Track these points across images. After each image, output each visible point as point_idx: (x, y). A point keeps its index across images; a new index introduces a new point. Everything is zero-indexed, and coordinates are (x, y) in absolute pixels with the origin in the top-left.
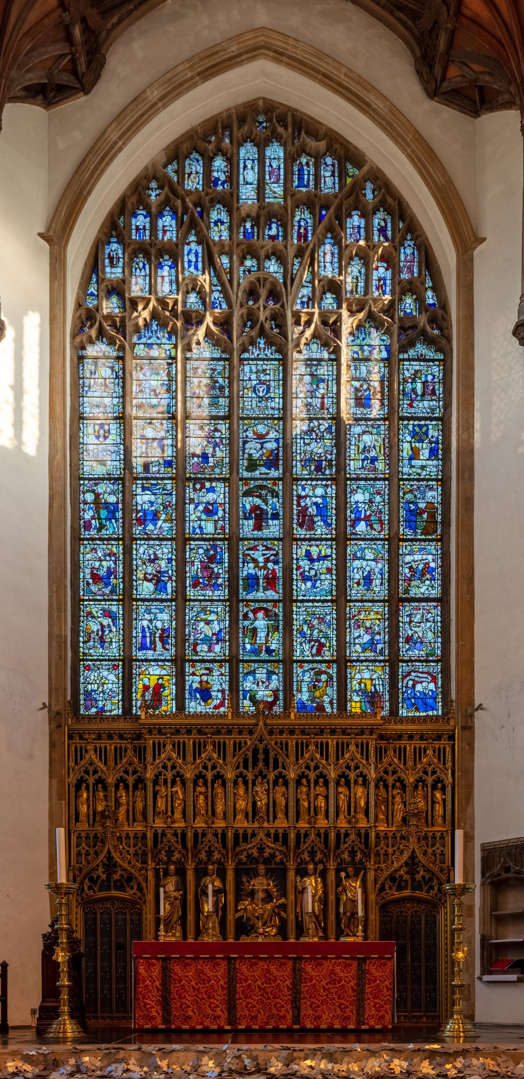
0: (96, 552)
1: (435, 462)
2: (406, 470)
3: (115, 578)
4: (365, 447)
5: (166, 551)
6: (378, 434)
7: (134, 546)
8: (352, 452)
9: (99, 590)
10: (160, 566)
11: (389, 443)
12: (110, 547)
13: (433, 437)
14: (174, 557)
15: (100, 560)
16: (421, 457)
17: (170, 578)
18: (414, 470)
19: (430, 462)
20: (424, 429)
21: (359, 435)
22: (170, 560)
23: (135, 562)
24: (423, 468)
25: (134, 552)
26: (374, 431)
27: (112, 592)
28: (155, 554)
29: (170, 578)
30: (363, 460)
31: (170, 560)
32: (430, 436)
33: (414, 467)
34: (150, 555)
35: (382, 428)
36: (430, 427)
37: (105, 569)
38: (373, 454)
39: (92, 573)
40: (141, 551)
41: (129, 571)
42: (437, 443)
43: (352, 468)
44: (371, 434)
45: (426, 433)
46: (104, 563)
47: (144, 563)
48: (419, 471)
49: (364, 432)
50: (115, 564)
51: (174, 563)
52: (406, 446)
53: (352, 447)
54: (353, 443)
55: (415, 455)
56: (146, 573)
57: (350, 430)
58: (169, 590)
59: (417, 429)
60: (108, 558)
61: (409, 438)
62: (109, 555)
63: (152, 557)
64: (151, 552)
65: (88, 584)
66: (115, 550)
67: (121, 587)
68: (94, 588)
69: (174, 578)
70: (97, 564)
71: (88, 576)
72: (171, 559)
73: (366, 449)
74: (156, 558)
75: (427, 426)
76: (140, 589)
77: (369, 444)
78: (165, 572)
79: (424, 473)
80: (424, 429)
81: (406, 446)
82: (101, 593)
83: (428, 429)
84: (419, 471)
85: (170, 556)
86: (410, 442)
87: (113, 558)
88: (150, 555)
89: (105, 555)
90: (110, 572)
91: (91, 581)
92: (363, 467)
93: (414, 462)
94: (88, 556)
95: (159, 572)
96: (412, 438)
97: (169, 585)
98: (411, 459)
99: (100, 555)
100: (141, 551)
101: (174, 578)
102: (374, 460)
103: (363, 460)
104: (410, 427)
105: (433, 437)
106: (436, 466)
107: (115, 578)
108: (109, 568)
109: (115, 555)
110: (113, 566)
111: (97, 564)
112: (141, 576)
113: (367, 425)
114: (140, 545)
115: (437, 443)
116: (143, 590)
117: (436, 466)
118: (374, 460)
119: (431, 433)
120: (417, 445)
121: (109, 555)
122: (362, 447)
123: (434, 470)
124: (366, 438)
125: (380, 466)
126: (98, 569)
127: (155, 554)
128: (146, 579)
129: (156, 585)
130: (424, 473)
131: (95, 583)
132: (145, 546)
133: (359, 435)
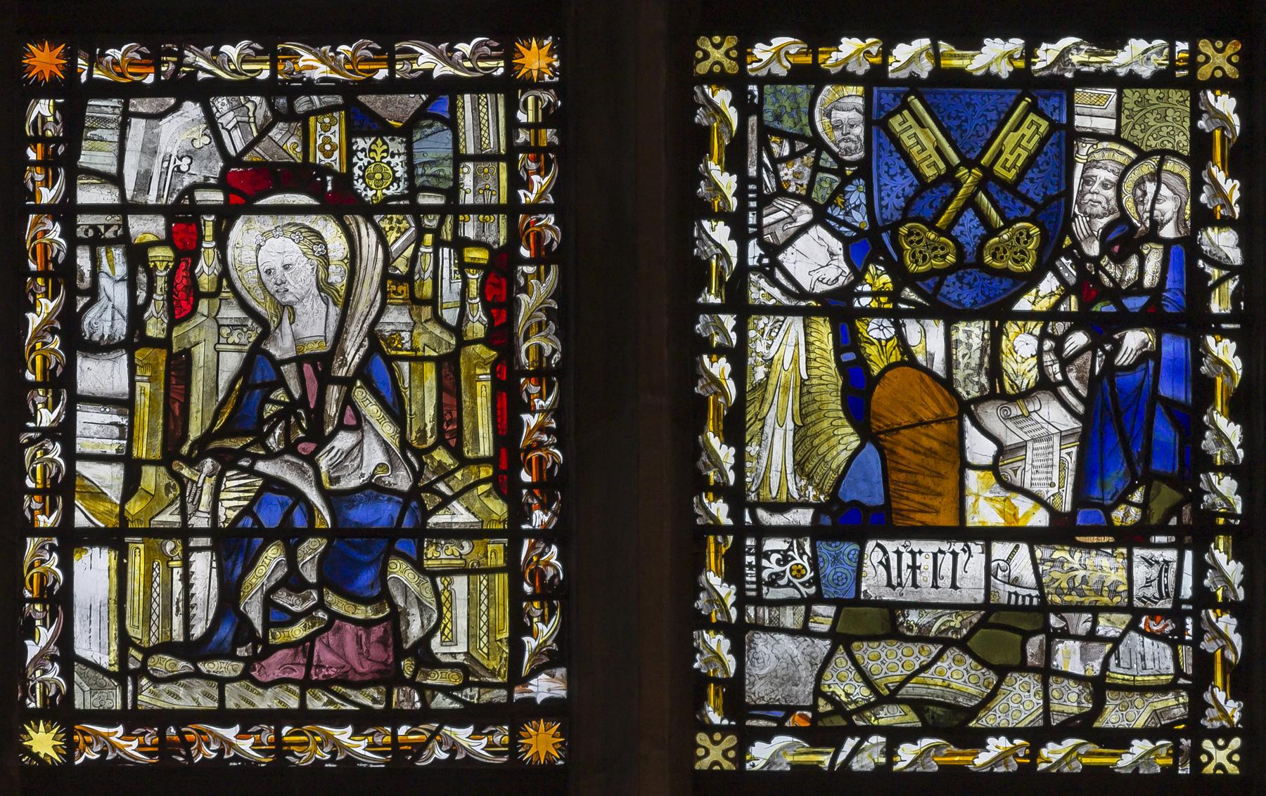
1: (1152, 569)
2: (779, 663)
4: (258, 370)
6: (428, 205)
8: (94, 429)
11: (563, 314)
13: (1125, 238)
16: (985, 510)
18: (889, 661)
19: (1102, 567)
20: (1017, 142)
21: (182, 216)
24: (1006, 632)
26: (379, 167)
30: (235, 547)
32: (1088, 230)
33: (887, 621)
35: (480, 122)
36: (1094, 112)
38: (364, 454)
42: (1184, 316)
43: (93, 643)
44: (341, 201)
45: (1045, 200)
48: (957, 677)
49: (248, 185)
52: (789, 351)
53: (101, 375)
54: (105, 319)
55: (896, 473)
57: (64, 160)
59: (923, 140)
61: (815, 260)
73: (276, 404)
75: (1056, 90)
77: (313, 323)
79: (1020, 702)
80: (1017, 142)
81: (789, 351)
83: (1064, 138)
84: (957, 677)
86: (837, 308)
92: (233, 633)
93: (880, 567)
96: (863, 248)
98: (848, 521)
102: (365, 544)
103: (235, 547)
104: (840, 116)
105: (1125, 238)
106: (1180, 617)
113: (283, 94)
115: (1184, 316)
117: (1180, 617)
118: (365, 544)
119: (1098, 185)
120: (927, 339)
122: (217, 360)
123: (1153, 657)
124: (266, 249)
125: (460, 616)
130: (1020, 702)
133: (182, 216)
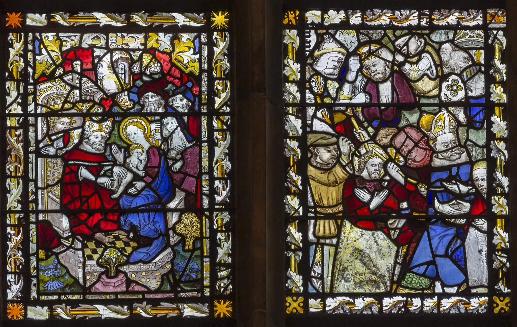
0: (91, 73)
3: (192, 205)
5: (457, 60)
7: (291, 37)
9: (108, 271)
10: (426, 141)
12: (164, 41)
14: (499, 94)
15: (110, 110)
17: (481, 205)
22: (477, 111)
23: (295, 123)
25: (293, 68)
27: (175, 282)
28: (398, 76)
29: (481, 205)
31: (477, 111)
34: (372, 85)
37: (137, 160)
39: (69, 183)
40: (327, 62)
41: (262, 167)
46: (133, 130)
47: (344, 129)
50: (191, 130)
51: (500, 126)
56: (352, 182)
58: (478, 269)
60: (152, 101)
62: (158, 85)
63: (386, 92)
64: (378, 67)
65: (49, 238)
66: (187, 57)
67: (223, 253)
68: (75, 261)
69: (500, 205)
70: (96, 134)
71: (49, 200)
72: (489, 108)
74: (408, 98)
76: (322, 263)
78: (451, 173)
82: (115, 285)
85: (478, 87)
87: (180, 103)
88: (372, 85)
89: (140, 85)
90: (162, 174)
91: (63, 224)
94: (48, 91)
95: (425, 172)
97: (476, 239)
99: (110, 84)
100: (327, 62)
101: (500, 205)
107: (192, 205)
108: (158, 153)
109: (187, 82)
110: (179, 140)
111: (96, 134)
112: (329, 195)
114: (325, 31)
116: (339, 271)
121: (158, 85)
126: (99, 162)
127: (398, 76)
128: (354, 212)
129: (406, 239)
131: (84, 231)
132: (349, 38)
